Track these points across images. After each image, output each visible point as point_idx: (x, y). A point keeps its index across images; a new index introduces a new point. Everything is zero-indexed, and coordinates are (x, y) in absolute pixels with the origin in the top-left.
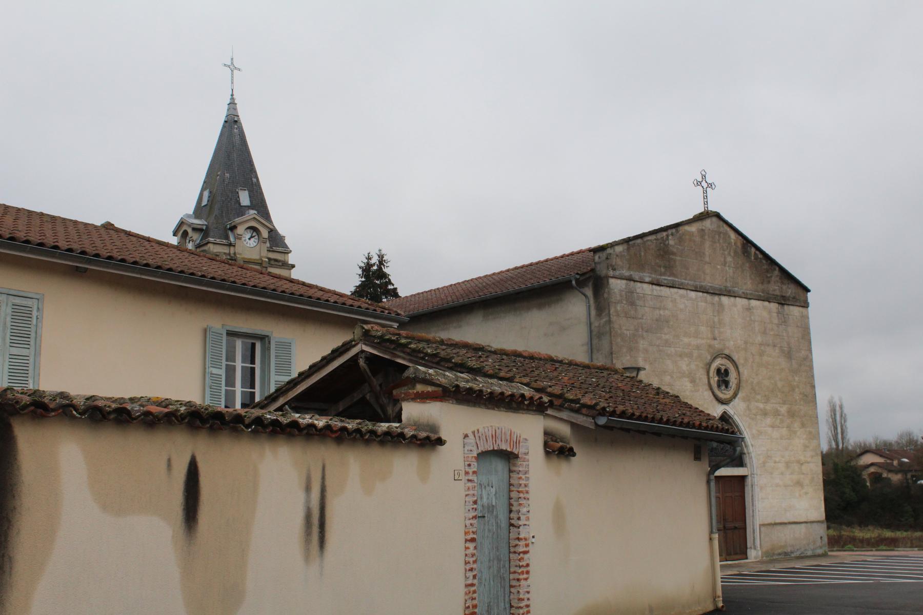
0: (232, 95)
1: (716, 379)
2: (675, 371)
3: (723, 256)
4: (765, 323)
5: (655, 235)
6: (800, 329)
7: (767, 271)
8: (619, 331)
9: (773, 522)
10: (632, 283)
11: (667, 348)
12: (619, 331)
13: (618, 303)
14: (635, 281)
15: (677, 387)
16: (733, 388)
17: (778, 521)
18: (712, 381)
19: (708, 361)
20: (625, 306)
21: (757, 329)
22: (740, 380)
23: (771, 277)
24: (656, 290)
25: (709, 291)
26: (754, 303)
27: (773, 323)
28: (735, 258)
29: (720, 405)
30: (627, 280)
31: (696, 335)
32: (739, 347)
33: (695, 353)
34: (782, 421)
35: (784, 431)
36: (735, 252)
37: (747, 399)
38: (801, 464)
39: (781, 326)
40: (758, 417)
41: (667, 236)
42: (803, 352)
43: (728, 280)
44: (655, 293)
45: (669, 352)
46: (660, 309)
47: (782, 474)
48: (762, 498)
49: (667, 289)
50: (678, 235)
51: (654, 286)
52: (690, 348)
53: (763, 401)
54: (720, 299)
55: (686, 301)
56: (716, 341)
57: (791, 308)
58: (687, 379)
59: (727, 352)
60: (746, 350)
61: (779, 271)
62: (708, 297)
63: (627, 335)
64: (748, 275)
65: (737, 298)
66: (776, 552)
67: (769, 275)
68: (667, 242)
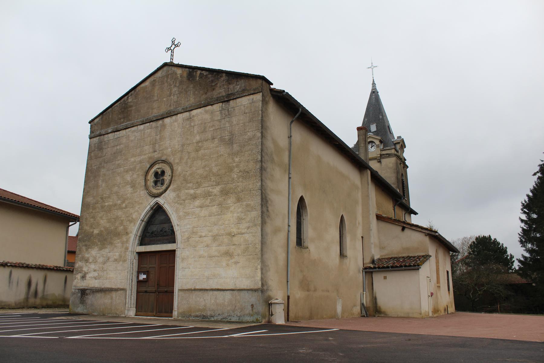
0: (373, 80)
7: (212, 81)
8: (90, 168)
9: (193, 288)
11: (118, 169)
12: (90, 168)
14: (104, 135)
15: (122, 193)
17: (197, 287)
21: (195, 131)
23: (217, 84)
24: (116, 135)
25: (152, 120)
26: (194, 112)
29: (153, 198)
30: (99, 136)
32: (176, 151)
35: (215, 209)
36: (181, 82)
38: (231, 235)
42: (249, 134)
44: (116, 137)
47: (207, 246)
48: (182, 268)
50: (136, 93)
51: (116, 133)
52: (135, 164)
53: (194, 187)
56: (155, 153)
57: (238, 100)
58: (129, 186)
59: (163, 158)
60: (182, 151)
62: (153, 124)
63: (94, 169)
66: (193, 314)
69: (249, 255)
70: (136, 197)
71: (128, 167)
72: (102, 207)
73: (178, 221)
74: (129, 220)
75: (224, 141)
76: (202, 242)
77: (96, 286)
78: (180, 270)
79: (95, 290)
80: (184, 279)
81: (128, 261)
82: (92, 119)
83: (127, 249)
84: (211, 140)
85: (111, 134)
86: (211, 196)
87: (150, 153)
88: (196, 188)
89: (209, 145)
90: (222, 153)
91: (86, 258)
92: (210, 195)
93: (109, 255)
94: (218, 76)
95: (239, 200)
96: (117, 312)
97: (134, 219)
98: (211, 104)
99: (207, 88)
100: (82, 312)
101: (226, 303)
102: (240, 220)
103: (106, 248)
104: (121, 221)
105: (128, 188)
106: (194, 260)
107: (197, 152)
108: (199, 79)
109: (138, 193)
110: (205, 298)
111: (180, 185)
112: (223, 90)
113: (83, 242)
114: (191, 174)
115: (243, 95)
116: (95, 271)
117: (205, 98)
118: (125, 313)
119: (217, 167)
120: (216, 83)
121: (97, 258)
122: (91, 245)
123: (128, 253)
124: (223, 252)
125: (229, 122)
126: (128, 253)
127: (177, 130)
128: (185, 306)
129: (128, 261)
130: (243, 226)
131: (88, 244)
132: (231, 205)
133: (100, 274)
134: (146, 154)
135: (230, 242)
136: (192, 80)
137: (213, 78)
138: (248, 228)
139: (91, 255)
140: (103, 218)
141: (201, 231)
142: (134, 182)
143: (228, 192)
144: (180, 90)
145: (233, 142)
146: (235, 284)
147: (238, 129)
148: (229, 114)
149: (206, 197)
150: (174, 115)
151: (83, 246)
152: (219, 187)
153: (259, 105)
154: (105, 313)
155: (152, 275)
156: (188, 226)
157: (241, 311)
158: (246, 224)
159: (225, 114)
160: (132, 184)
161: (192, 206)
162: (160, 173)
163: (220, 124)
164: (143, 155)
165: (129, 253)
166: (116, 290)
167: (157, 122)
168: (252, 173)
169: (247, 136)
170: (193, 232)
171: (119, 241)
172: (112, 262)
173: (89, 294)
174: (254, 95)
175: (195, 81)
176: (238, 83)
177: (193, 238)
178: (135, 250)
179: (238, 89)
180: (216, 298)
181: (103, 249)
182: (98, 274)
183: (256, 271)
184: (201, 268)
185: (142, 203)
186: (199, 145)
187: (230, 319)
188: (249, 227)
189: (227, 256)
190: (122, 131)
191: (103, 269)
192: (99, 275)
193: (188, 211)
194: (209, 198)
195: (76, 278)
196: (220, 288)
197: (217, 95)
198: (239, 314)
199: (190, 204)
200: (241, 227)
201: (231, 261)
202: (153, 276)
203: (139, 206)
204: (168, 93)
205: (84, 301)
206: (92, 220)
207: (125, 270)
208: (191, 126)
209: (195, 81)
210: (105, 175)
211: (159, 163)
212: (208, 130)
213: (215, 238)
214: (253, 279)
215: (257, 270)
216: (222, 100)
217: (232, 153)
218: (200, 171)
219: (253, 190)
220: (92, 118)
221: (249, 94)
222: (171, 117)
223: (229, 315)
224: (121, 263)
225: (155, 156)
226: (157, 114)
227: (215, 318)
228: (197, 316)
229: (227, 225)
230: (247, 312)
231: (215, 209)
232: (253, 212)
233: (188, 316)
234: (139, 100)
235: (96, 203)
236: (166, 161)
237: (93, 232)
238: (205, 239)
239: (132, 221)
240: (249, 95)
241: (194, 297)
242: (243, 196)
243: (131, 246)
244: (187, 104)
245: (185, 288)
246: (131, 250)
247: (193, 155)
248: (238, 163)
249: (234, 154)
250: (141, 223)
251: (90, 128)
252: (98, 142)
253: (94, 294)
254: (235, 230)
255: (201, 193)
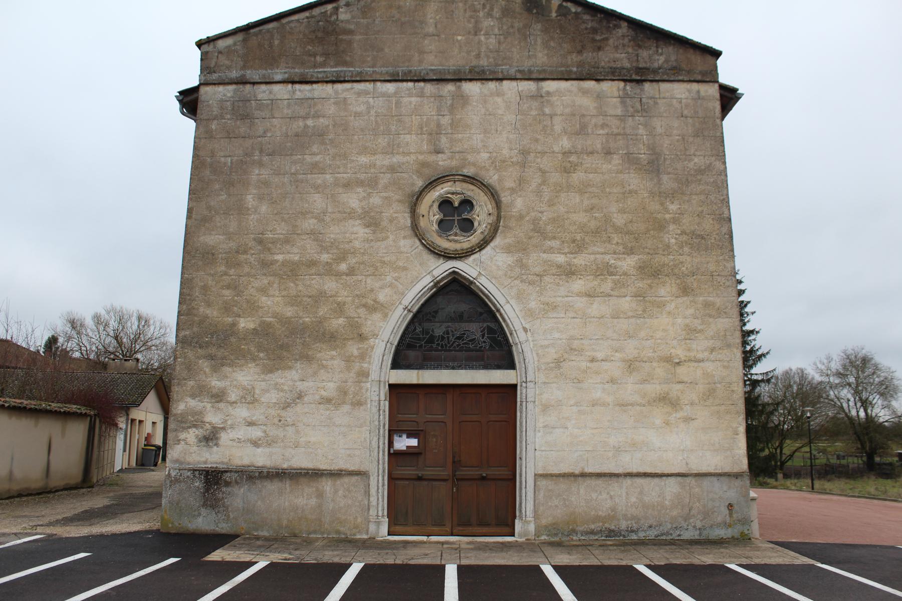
1: (438, 217)
2: (330, 210)
3: (473, 20)
4: (583, 116)
5: (310, 11)
6: (690, 120)
7: (594, 31)
8: (209, 160)
9: (577, 472)
10: (248, 87)
11: (313, 176)
12: (209, 160)
13: (214, 119)
14: (254, 83)
15: (332, 236)
16: (479, 231)
18: (423, 223)
19: (417, 189)
20: (229, 122)
22: (499, 218)
23: (607, 39)
24: (300, 90)
26: (550, 86)
27: (606, 115)
28: (504, 20)
29: (441, 261)
30: (236, 83)
31: (390, 149)
32: (504, 161)
33: (385, 179)
34: (617, 285)
35: (626, 303)
37: (519, 248)
39: (630, 118)
40: (547, 279)
41: (336, 9)
42: (696, 160)
43: (483, 54)
44: (298, 95)
45: (319, 181)
46: (305, 118)
48: (545, 427)
49: (329, 88)
51: (297, 86)
53: (566, 250)
54: (459, 87)
55: (371, 100)
56: (440, 155)
57: (664, 86)
58: (358, 222)
59: (469, 171)
60: (523, 165)
61: (629, 27)
62: (429, 88)
63: (225, 164)
64: (539, 41)
65: (505, 82)
66: (581, 529)
67: (598, 38)
68: (334, 18)
69: (717, 405)
70: (384, 251)
71: (349, 175)
72: (265, 264)
73: (525, 320)
74: (365, 306)
75: (635, 164)
76: (597, 373)
77: (260, 464)
78: (539, 431)
79: (257, 474)
80: (552, 452)
81: (369, 405)
82: (208, 37)
83: (364, 374)
84: (603, 155)
85: (282, 84)
86: (615, 275)
87: (421, 153)
88: (572, 254)
89: (597, 164)
90: (631, 187)
91: (214, 391)
92: (612, 272)
93: (301, 386)
94: (609, 22)
95: (685, 290)
96: (342, 529)
97: (382, 305)
98: (599, 78)
99: (581, 41)
100: (212, 527)
101: (667, 502)
102: (691, 332)
103: (290, 368)
104: (338, 305)
105: (354, 225)
106: (579, 411)
107: (566, 175)
108: (557, 16)
109: (390, 241)
110: (612, 493)
111: (525, 240)
112: (623, 55)
113: (200, 348)
114: (554, 220)
115: (677, 78)
116: (251, 424)
117: (576, 61)
118: (367, 531)
119: (625, 216)
120: (604, 36)
121: (257, 391)
122: (232, 357)
123: (369, 386)
124: (654, 395)
125: (646, 125)
126: (368, 385)
127: (502, 115)
128: (559, 511)
129: (369, 405)
130: (700, 346)
131: (220, 353)
132: (668, 299)
133: (271, 434)
134: (411, 153)
135: (670, 376)
136: (537, 13)
137: (595, 25)
138: (712, 350)
139: (235, 383)
140: (271, 292)
141: (593, 347)
142: (372, 214)
143: (658, 272)
144: (505, 27)
145: (661, 170)
146: (687, 464)
147: (671, 145)
148: (643, 110)
149: (602, 275)
150: (492, 80)
151: (199, 358)
152: (636, 258)
153: (714, 108)
154: (297, 532)
155: (434, 440)
156: (557, 335)
157: (705, 518)
158: (706, 341)
159: (633, 107)
160: (367, 218)
161: (562, 291)
162: (456, 204)
163: (623, 126)
164: (397, 153)
165: (371, 384)
166: (336, 474)
167: (438, 84)
168: (713, 241)
169: (692, 163)
170: (572, 349)
171: (334, 353)
172: (313, 406)
173: (237, 483)
174: (700, 84)
175: (548, 18)
176: (660, 51)
177: (573, 362)
178: (387, 379)
179: (660, 62)
180: (641, 493)
181: (278, 369)
182: (265, 432)
183: (736, 436)
184: (595, 428)
185: (405, 269)
186: (571, 159)
187: (679, 535)
188: (714, 348)
189: (665, 404)
190: (319, 85)
191: (280, 421)
192: (267, 436)
193: (552, 300)
194: (610, 277)
195: (179, 440)
196: (649, 472)
197: (609, 62)
198: (699, 524)
199: (558, 285)
200: (694, 346)
201: (674, 415)
202: (436, 442)
203: (396, 274)
204: (471, 25)
205: (217, 500)
206: (227, 292)
207: (361, 426)
208: (544, 114)
209: (548, 18)
210: (266, 184)
211: (455, 182)
212: (593, 132)
213: (631, 365)
214: (729, 453)
215: (737, 434)
216: (627, 75)
217: (660, 193)
218: (580, 217)
219: (718, 275)
220: (212, 33)
221: (693, 79)
222: (483, 82)
223: (674, 526)
224: (346, 408)
225: (440, 163)
226: (439, 66)
227: (642, 535)
228: (592, 532)
229: (659, 341)
230: (719, 519)
231: (626, 303)
232: (721, 320)
233: (566, 533)
234: (377, 22)
235: (237, 252)
236: (477, 180)
237: (234, 325)
238: (606, 366)
239: (375, 307)
240: (690, 81)
241: (582, 491)
242: (695, 285)
243: (378, 367)
244: (527, 64)
245: (556, 471)
246: (378, 379)
247: (555, 177)
248: (677, 215)
249: (665, 195)
250: (406, 315)
251: (202, 60)
252: (232, 97)
253: (255, 483)
254: (680, 353)
255: (585, 265)
